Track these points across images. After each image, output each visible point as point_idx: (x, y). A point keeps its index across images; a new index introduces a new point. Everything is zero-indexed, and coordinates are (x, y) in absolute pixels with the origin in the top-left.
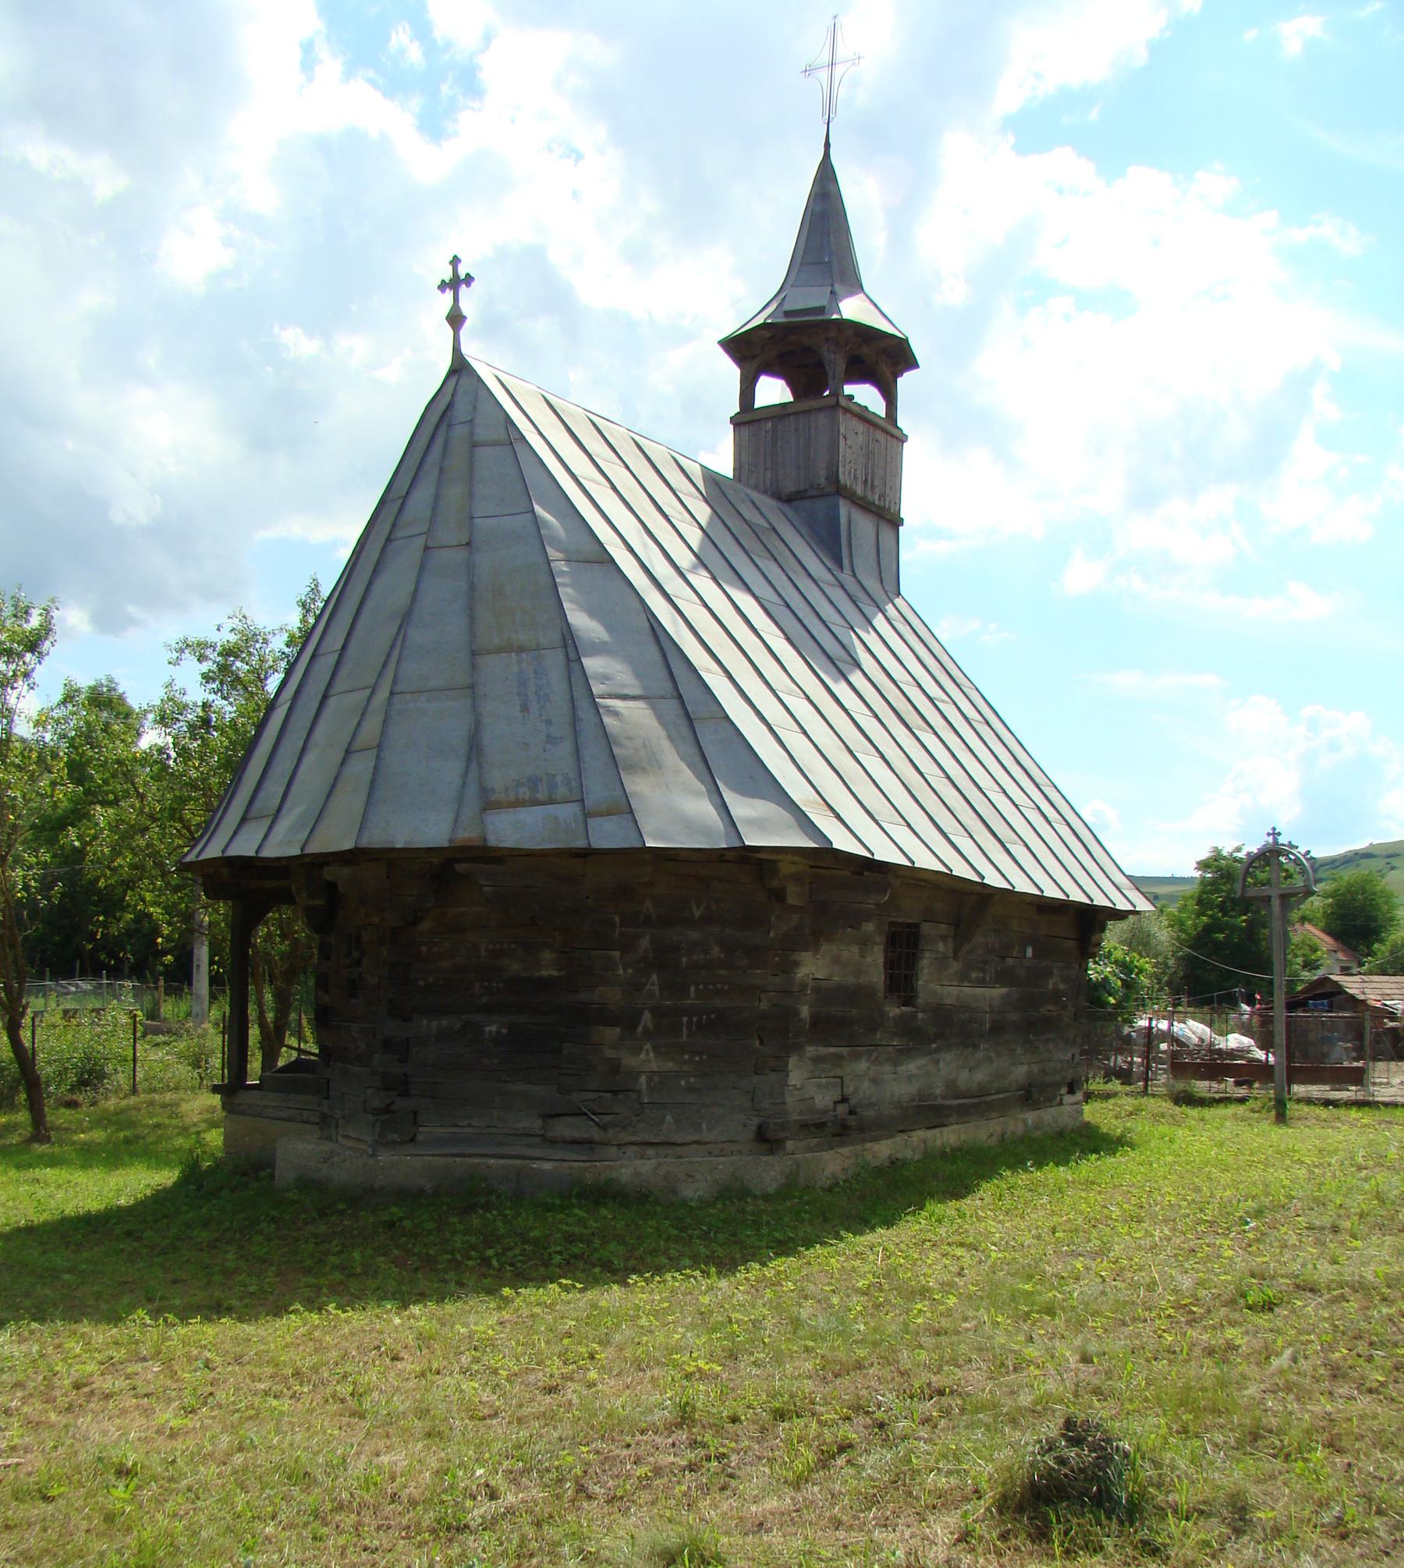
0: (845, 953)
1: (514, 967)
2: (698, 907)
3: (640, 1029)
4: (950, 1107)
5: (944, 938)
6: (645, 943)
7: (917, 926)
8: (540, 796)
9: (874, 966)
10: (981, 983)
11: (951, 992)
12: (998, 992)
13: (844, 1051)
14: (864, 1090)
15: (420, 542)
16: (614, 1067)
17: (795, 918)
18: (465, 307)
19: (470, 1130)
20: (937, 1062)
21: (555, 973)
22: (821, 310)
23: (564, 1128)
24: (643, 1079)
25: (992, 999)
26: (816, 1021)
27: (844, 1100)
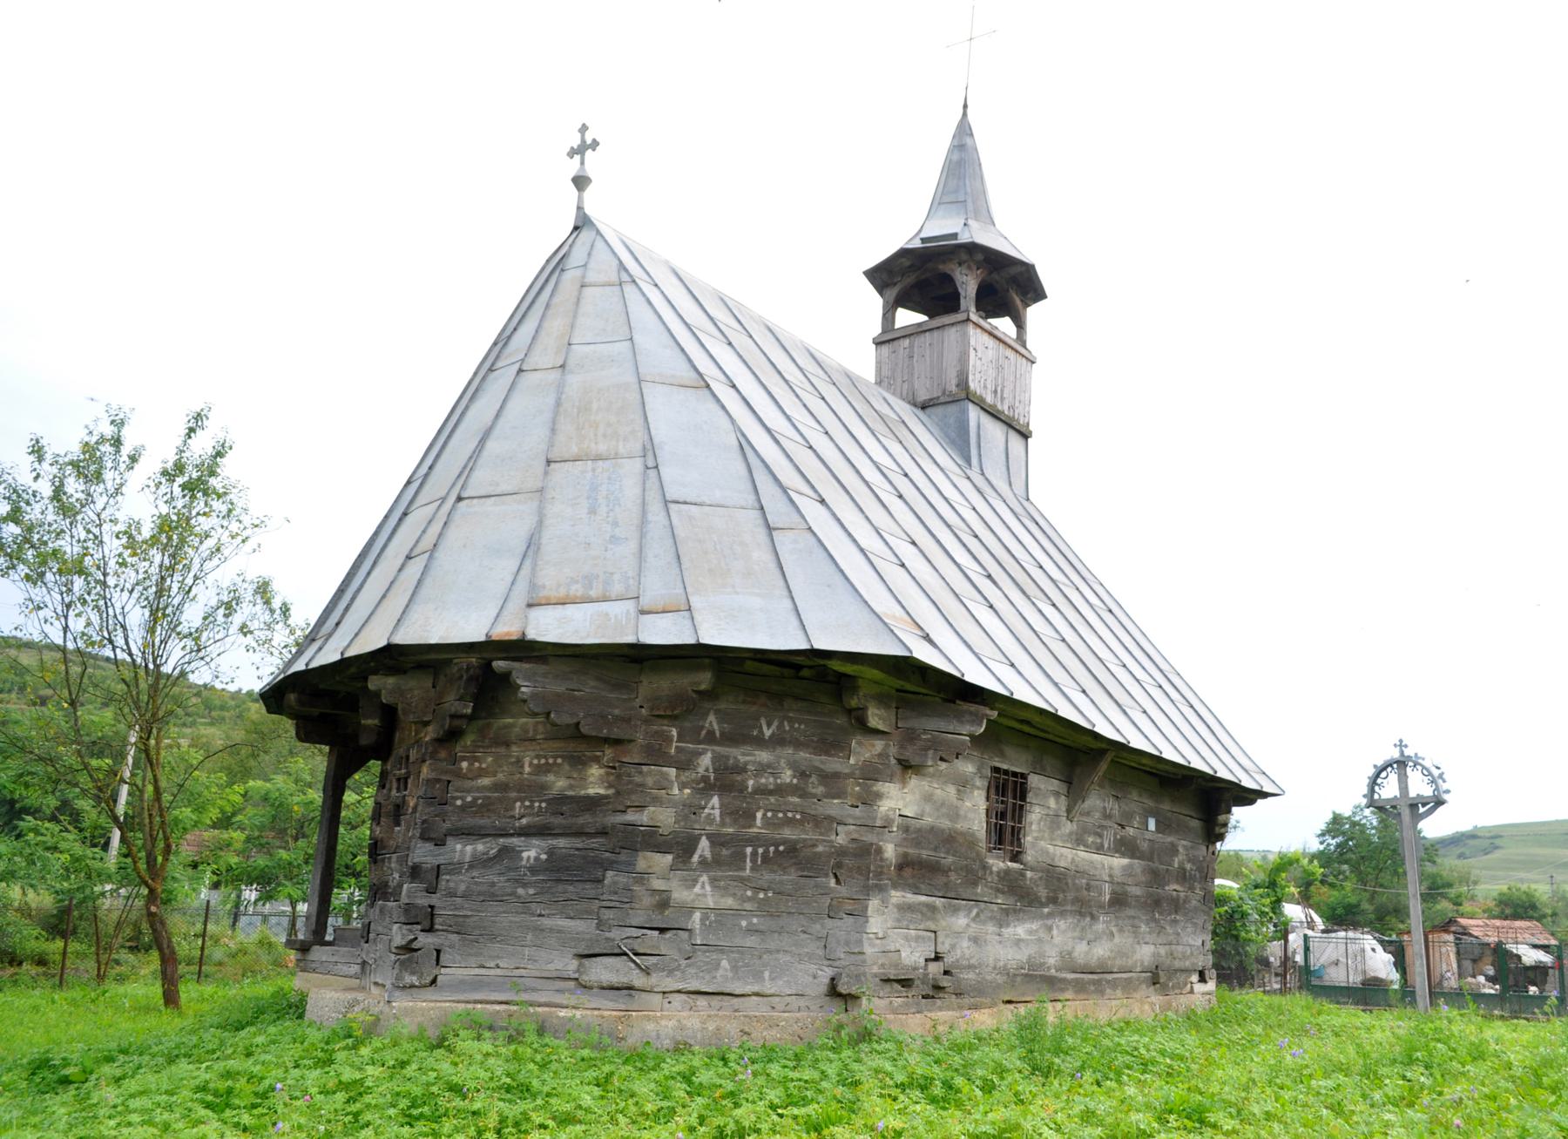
0: (939, 792)
1: (559, 784)
2: (769, 726)
3: (695, 858)
4: (1064, 980)
5: (1057, 794)
6: (706, 761)
7: (1023, 776)
8: (593, 593)
9: (974, 813)
10: (1099, 849)
11: (1065, 855)
12: (1119, 862)
13: (939, 902)
14: (961, 951)
15: (517, 367)
16: (664, 903)
17: (879, 745)
18: (590, 171)
19: (499, 972)
20: (1050, 929)
21: (602, 791)
22: (955, 236)
23: (604, 971)
24: (697, 916)
25: (1111, 868)
26: (904, 864)
27: (937, 958)
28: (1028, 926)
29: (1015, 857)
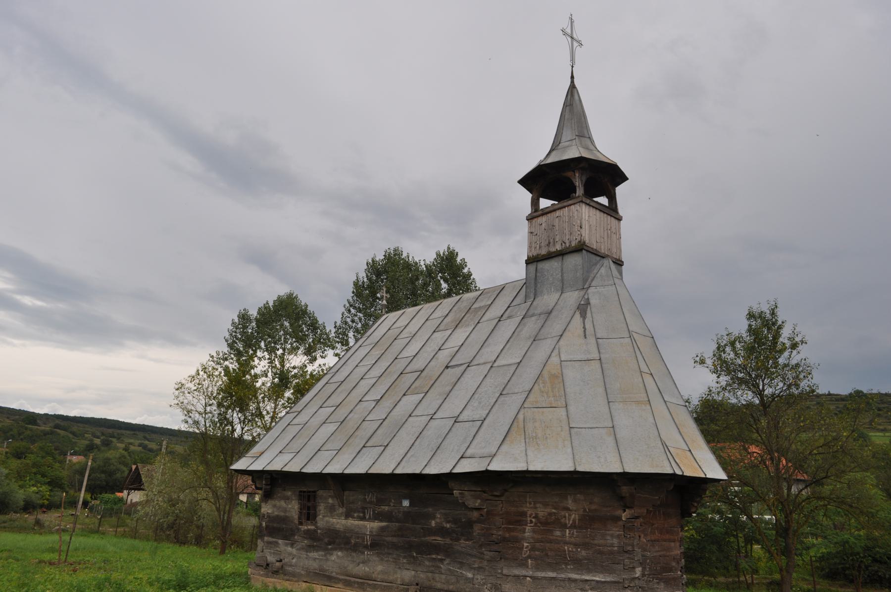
7: (314, 492)
10: (363, 519)
11: (340, 522)
28: (321, 553)
29: (315, 525)
